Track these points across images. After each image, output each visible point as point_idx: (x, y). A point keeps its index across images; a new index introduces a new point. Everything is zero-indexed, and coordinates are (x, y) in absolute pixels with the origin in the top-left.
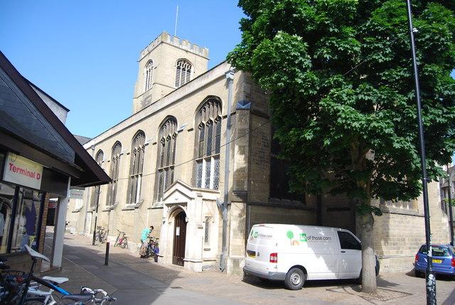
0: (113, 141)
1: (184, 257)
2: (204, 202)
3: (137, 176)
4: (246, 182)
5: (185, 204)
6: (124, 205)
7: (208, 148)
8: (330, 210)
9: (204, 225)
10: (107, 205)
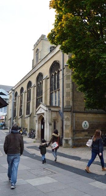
2: (53, 112)
5: (43, 114)
6: (26, 116)
7: (54, 87)
9: (53, 124)
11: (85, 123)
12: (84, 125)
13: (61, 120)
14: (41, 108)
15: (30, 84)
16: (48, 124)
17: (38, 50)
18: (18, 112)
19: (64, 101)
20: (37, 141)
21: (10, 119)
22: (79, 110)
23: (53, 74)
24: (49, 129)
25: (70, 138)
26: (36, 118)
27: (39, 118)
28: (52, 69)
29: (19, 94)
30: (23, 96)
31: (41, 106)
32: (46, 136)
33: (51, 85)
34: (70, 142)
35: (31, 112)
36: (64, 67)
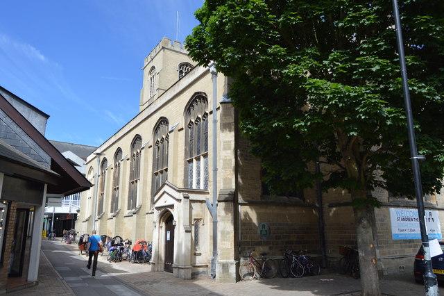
0: (114, 149)
1: (172, 263)
3: (136, 181)
5: (172, 206)
6: (127, 212)
7: (197, 147)
10: (112, 212)
12: (261, 231)
14: (165, 194)
18: (107, 204)
19: (218, 179)
27: (162, 216)
28: (189, 108)
30: (121, 166)
31: (166, 188)
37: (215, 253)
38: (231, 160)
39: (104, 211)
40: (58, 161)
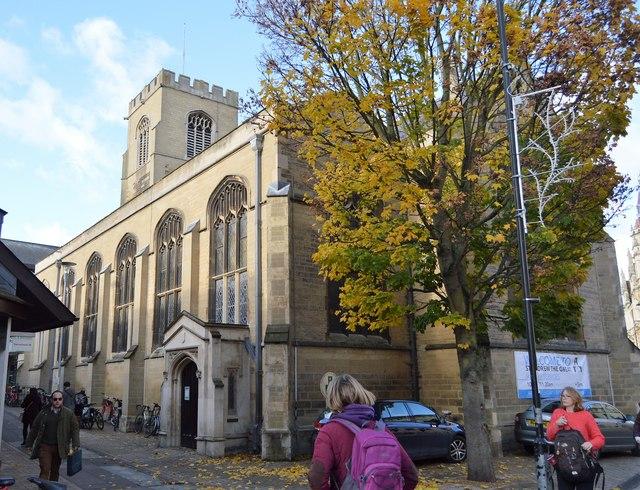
2: (225, 345)
4: (287, 311)
5: (194, 350)
6: (110, 355)
8: (431, 348)
9: (226, 382)
11: (330, 379)
13: (252, 369)
14: (183, 331)
15: (127, 245)
16: (211, 385)
17: (144, 120)
18: (75, 342)
19: (265, 308)
20: (168, 444)
21: (41, 367)
22: (310, 339)
23: (222, 218)
24: (216, 401)
25: (286, 429)
26: (157, 369)
29: (80, 274)
31: (184, 321)
32: (205, 425)
33: (213, 253)
34: (287, 443)
35: (133, 339)
36: (264, 198)
37: (260, 420)
38: (282, 281)
39: (70, 353)
40: (28, 283)
